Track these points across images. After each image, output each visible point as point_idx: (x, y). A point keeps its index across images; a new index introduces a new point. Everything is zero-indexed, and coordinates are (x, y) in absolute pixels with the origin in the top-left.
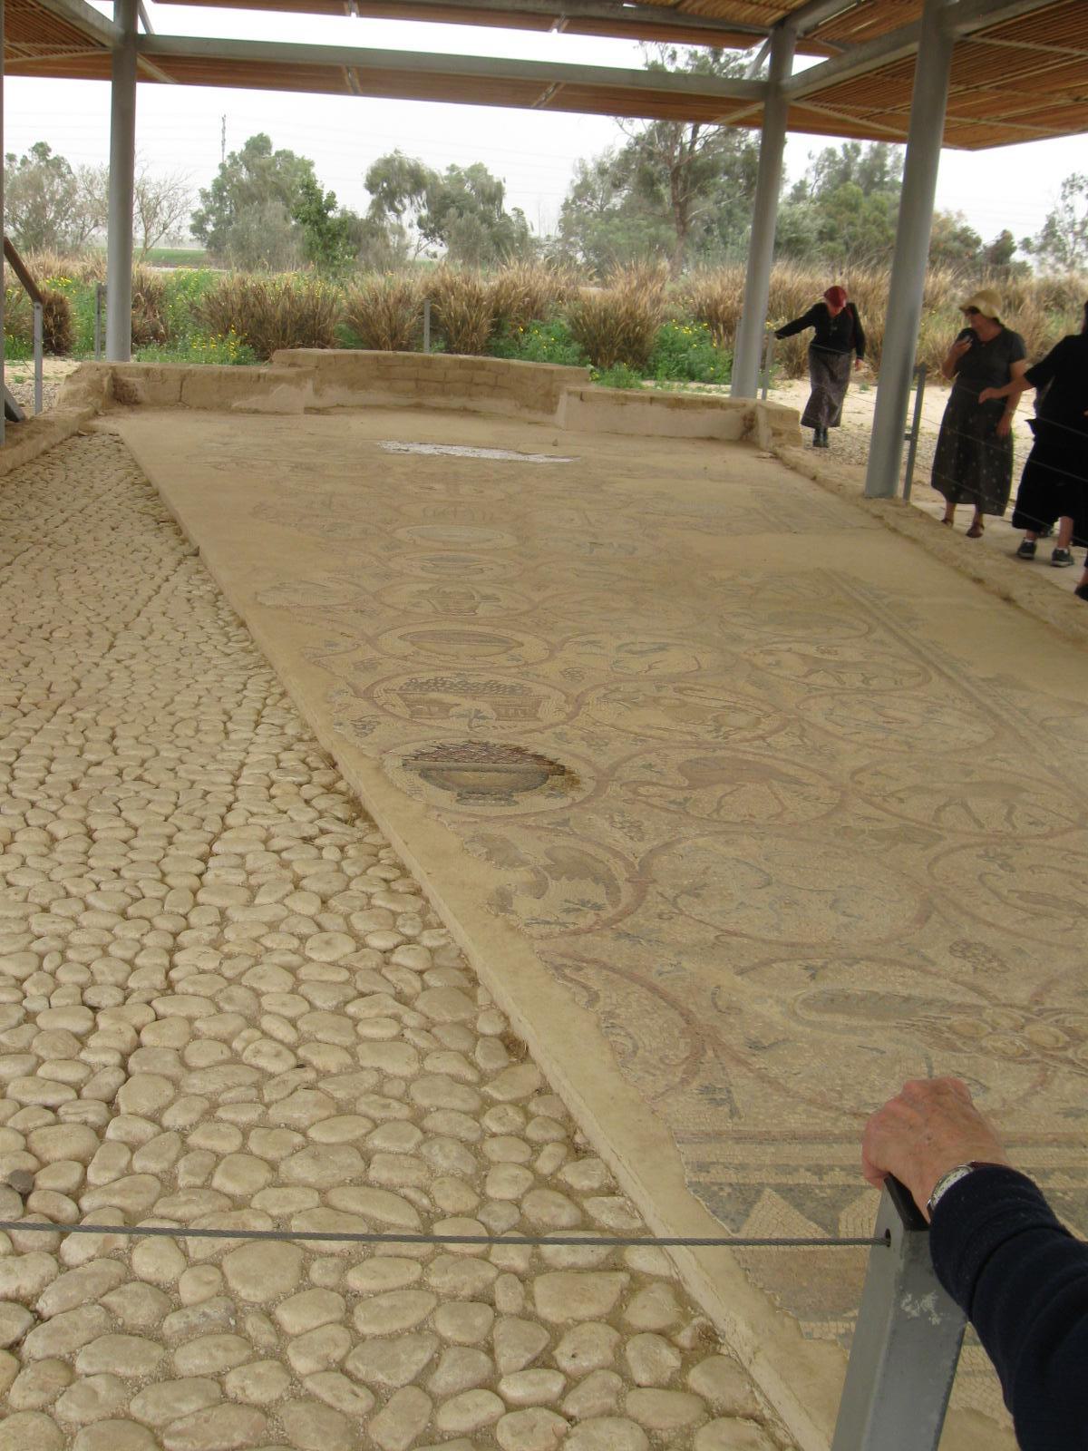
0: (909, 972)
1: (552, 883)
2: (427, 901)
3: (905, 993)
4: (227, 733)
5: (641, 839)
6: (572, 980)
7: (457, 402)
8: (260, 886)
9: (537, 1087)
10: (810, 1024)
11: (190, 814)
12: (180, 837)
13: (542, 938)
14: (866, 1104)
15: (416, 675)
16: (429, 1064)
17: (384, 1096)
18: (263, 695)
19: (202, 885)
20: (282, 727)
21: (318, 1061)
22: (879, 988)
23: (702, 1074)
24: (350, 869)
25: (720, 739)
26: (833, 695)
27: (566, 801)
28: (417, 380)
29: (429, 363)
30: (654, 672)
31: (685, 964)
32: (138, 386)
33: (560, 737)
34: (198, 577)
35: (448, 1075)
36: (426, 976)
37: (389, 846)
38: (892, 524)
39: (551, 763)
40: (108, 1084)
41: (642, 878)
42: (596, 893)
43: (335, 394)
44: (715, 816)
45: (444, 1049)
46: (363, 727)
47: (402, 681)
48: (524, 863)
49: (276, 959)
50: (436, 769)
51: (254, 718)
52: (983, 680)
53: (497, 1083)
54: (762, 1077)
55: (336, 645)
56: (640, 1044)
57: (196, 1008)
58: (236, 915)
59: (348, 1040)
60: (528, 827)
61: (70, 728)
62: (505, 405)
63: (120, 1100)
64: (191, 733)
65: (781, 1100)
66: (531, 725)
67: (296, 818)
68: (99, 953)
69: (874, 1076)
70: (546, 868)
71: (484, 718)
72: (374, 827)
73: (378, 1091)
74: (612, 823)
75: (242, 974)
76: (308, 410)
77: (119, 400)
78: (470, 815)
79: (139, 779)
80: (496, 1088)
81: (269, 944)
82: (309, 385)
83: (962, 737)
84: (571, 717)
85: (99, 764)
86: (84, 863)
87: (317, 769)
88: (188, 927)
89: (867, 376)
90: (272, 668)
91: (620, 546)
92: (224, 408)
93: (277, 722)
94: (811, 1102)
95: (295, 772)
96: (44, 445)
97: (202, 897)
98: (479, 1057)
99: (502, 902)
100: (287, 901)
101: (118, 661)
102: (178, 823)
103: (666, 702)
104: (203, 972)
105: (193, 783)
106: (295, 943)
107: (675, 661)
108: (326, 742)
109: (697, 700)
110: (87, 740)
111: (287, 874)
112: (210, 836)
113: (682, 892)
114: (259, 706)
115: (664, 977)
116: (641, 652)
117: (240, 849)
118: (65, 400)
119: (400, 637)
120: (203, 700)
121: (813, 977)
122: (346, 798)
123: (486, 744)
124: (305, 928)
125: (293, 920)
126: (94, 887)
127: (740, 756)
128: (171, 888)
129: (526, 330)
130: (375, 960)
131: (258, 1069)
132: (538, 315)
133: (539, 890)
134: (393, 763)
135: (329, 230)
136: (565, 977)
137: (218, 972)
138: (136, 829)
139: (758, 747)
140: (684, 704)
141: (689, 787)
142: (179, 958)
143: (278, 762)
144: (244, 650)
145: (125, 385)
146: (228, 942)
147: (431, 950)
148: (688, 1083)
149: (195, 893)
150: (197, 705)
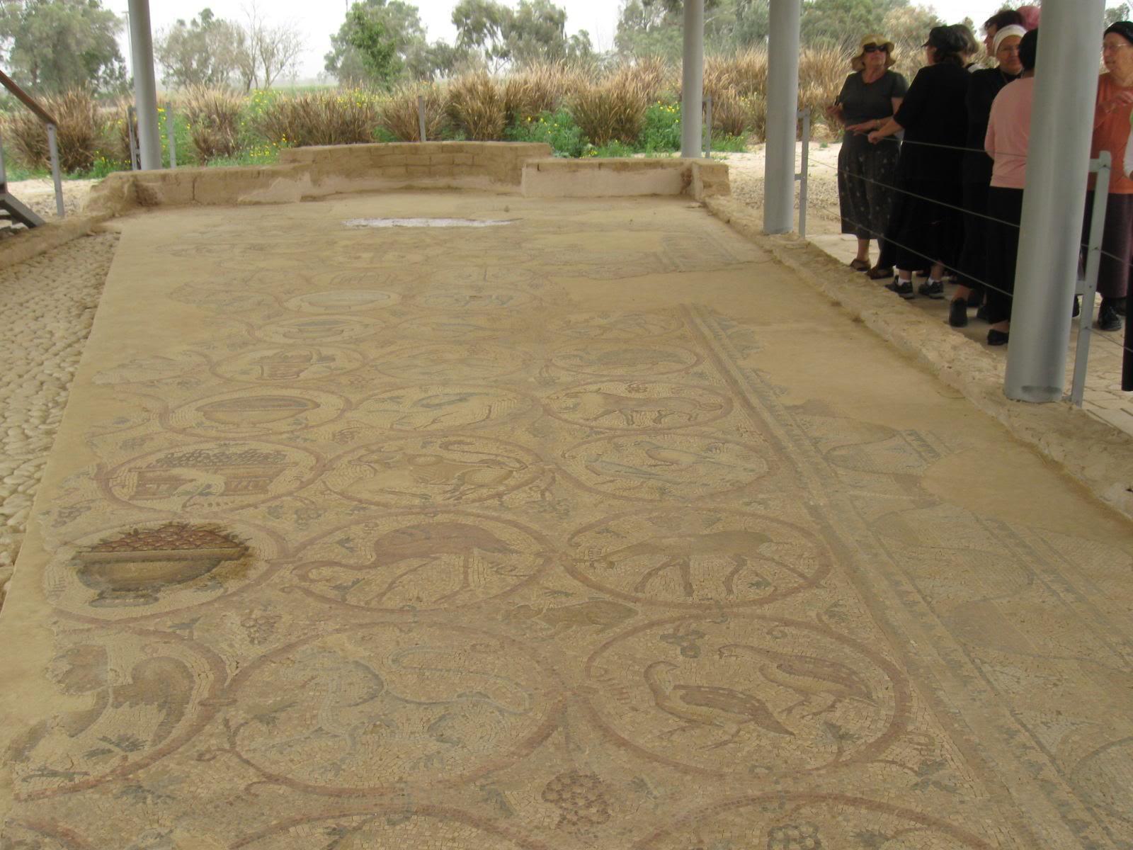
7: (442, 182)
26: (610, 439)
28: (406, 165)
29: (416, 151)
32: (157, 190)
38: (779, 258)
43: (332, 182)
52: (787, 408)
62: (482, 181)
76: (305, 198)
77: (141, 203)
82: (307, 177)
89: (827, 136)
92: (231, 203)
96: (43, 246)
116: (437, 405)
118: (88, 206)
129: (537, 120)
132: (550, 107)
135: (380, 52)
139: (487, 508)
145: (146, 190)
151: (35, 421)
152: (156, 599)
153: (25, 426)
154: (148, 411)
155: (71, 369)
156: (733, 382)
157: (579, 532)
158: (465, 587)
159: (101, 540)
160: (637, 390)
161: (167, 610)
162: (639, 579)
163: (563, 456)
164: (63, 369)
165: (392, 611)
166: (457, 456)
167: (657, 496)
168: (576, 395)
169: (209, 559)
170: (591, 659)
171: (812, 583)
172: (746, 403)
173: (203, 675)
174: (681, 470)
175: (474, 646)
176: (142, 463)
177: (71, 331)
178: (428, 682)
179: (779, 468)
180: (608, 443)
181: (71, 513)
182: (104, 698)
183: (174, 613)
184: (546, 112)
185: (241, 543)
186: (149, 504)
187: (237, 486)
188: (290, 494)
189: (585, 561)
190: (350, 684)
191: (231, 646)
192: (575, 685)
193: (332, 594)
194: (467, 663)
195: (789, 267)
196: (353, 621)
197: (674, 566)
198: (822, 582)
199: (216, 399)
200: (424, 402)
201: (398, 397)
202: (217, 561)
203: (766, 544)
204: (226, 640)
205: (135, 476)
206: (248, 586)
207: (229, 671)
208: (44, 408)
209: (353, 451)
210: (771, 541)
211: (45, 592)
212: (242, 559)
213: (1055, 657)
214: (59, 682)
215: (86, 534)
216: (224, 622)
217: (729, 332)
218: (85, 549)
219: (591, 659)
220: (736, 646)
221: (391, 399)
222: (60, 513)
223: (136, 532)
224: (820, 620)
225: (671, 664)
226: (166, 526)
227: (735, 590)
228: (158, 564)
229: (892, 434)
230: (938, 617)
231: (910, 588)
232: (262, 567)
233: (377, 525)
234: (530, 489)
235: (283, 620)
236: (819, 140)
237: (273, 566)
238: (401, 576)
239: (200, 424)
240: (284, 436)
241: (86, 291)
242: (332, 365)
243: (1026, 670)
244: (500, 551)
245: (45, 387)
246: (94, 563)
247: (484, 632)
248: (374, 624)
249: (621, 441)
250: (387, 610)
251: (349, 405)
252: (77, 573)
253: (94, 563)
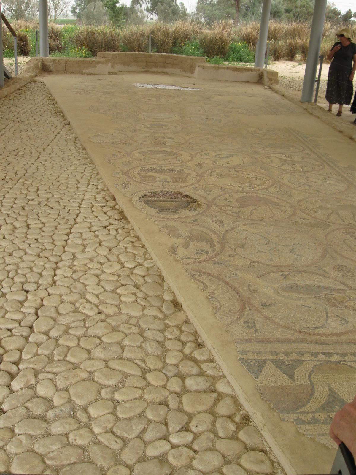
0: (319, 277)
1: (191, 243)
2: (147, 250)
3: (318, 284)
4: (77, 188)
5: (223, 226)
6: (198, 280)
7: (160, 70)
8: (87, 245)
9: (185, 320)
10: (284, 296)
11: (64, 218)
12: (59, 227)
13: (187, 264)
14: (304, 328)
15: (144, 167)
16: (146, 312)
17: (130, 324)
18: (91, 174)
19: (67, 244)
20: (97, 186)
21: (106, 311)
22: (309, 283)
23: (244, 316)
24: (119, 238)
25: (251, 189)
26: (291, 173)
27: (197, 212)
29: (150, 56)
30: (228, 165)
31: (239, 274)
32: (51, 65)
33: (195, 188)
34: (70, 132)
35: (153, 316)
36: (146, 278)
37: (133, 229)
38: (311, 112)
39: (191, 198)
40: (30, 320)
41: (223, 241)
42: (207, 247)
43: (118, 67)
44: (249, 218)
45: (152, 306)
46: (125, 186)
47: (139, 169)
48: (181, 236)
49: (92, 272)
50: (150, 201)
51: (87, 182)
53: (170, 319)
54: (266, 318)
55: (116, 156)
56: (222, 304)
57: (63, 291)
58: (78, 255)
59: (117, 303)
60: (183, 222)
61: (23, 187)
62: (177, 71)
63: (34, 326)
64: (65, 188)
65: (273, 326)
66: (184, 184)
67: (101, 219)
68: (29, 270)
69: (307, 317)
70: (189, 237)
71: (168, 182)
72: (128, 222)
73: (127, 322)
74: (213, 220)
75: (80, 278)
76: (109, 73)
78: (163, 218)
79: (46, 205)
80: (170, 321)
81: (90, 266)
82: (109, 64)
83: (337, 188)
84: (199, 181)
85: (32, 200)
86: (25, 237)
87: (109, 201)
88: (62, 260)
89: (301, 60)
90: (94, 164)
91: (216, 119)
92: (80, 73)
93: (95, 184)
94: (284, 327)
95: (101, 202)
96: (18, 87)
97: (67, 249)
98: (164, 309)
99: (173, 250)
100: (97, 250)
101: (41, 163)
102: (59, 221)
104: (66, 277)
105: (65, 206)
106: (99, 266)
107: (235, 161)
108: (112, 191)
109: (243, 175)
110: (28, 191)
111: (97, 240)
112: (70, 226)
113: (238, 246)
114: (89, 178)
115: (231, 278)
116: (223, 157)
117: (80, 231)
119: (139, 153)
120: (70, 176)
121: (284, 278)
122: (118, 212)
123: (168, 191)
124: (103, 260)
125: (99, 257)
126: (28, 246)
127: (258, 195)
128: (56, 246)
129: (184, 45)
130: (128, 272)
131: (85, 314)
132: (189, 39)
133: (186, 246)
134: (135, 199)
135: (117, 11)
136: (195, 279)
137: (71, 277)
138: (44, 224)
140: (238, 176)
141: (241, 207)
142: (58, 272)
143: (95, 198)
144: (85, 158)
145: (46, 65)
146: (75, 266)
147: (147, 268)
148: (240, 320)
149: (64, 247)
150: (68, 178)
184: (188, 42)
195: (316, 116)
200: (218, 156)
236: (298, 61)
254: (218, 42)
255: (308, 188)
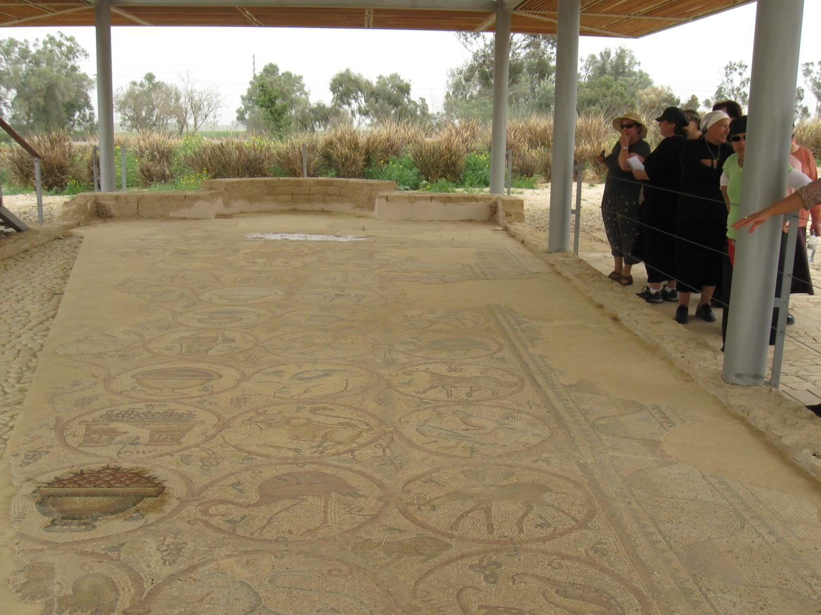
7: (317, 206)
25: (317, 455)
26: (435, 408)
29: (299, 184)
32: (111, 207)
38: (559, 270)
43: (238, 205)
52: (565, 386)
76: (219, 216)
82: (220, 201)
83: (522, 440)
89: (594, 178)
92: (165, 218)
96: (26, 246)
103: (294, 422)
116: (308, 379)
118: (61, 217)
127: (324, 470)
129: (387, 162)
132: (396, 153)
135: (276, 111)
139: (343, 460)
145: (103, 206)
151: (12, 381)
152: (94, 527)
153: (5, 384)
154: (96, 377)
155: (41, 341)
156: (525, 366)
157: (410, 481)
158: (324, 523)
159: (56, 478)
160: (455, 371)
161: (102, 536)
162: (454, 520)
163: (400, 421)
164: (34, 341)
165: (270, 541)
166: (321, 419)
167: (468, 454)
168: (409, 373)
169: (135, 496)
170: (417, 583)
171: (582, 525)
172: (535, 382)
173: (126, 589)
174: (486, 434)
175: (330, 570)
176: (89, 418)
177: (42, 311)
178: (295, 599)
179: (558, 434)
180: (434, 411)
181: (34, 455)
182: (50, 606)
183: (108, 538)
184: (394, 157)
185: (159, 484)
186: (92, 450)
187: (158, 438)
188: (197, 445)
189: (414, 505)
190: (236, 599)
191: (148, 566)
192: (405, 604)
193: (226, 527)
194: (324, 584)
196: (240, 549)
197: (480, 509)
198: (590, 525)
199: (146, 369)
200: (299, 376)
201: (280, 372)
202: (141, 497)
203: (548, 494)
204: (145, 561)
205: (83, 428)
206: (164, 517)
207: (146, 586)
208: (19, 371)
209: (245, 413)
210: (552, 491)
211: (11, 518)
212: (159, 498)
213: (762, 587)
214: (17, 591)
215: (44, 473)
216: (140, 546)
217: (522, 327)
218: (43, 485)
219: (417, 583)
220: (525, 574)
221: (275, 372)
222: (26, 455)
223: (82, 472)
224: (588, 555)
225: (476, 589)
226: (104, 469)
227: (525, 530)
228: (96, 499)
229: (641, 407)
230: (675, 553)
231: (653, 530)
232: (174, 503)
233: (261, 472)
234: (375, 446)
235: (188, 546)
236: (588, 181)
237: (183, 503)
238: (277, 513)
239: (133, 389)
240: (195, 400)
241: (56, 281)
242: (233, 345)
243: (740, 597)
244: (351, 495)
245: (21, 355)
246: (49, 496)
247: (338, 560)
248: (256, 551)
249: (443, 410)
250: (265, 540)
251: (244, 377)
252: (36, 503)
253: (49, 496)
254: (443, 156)
255: (453, 443)
